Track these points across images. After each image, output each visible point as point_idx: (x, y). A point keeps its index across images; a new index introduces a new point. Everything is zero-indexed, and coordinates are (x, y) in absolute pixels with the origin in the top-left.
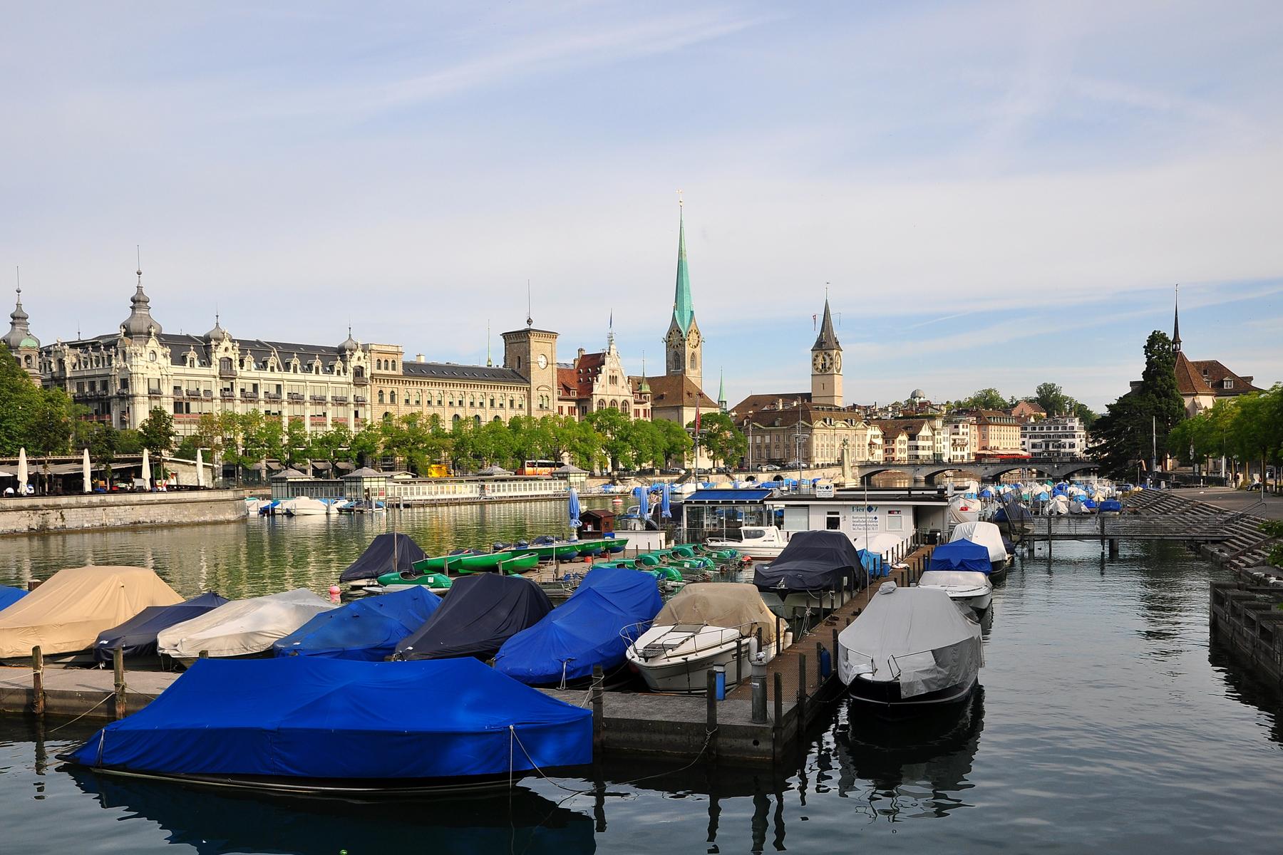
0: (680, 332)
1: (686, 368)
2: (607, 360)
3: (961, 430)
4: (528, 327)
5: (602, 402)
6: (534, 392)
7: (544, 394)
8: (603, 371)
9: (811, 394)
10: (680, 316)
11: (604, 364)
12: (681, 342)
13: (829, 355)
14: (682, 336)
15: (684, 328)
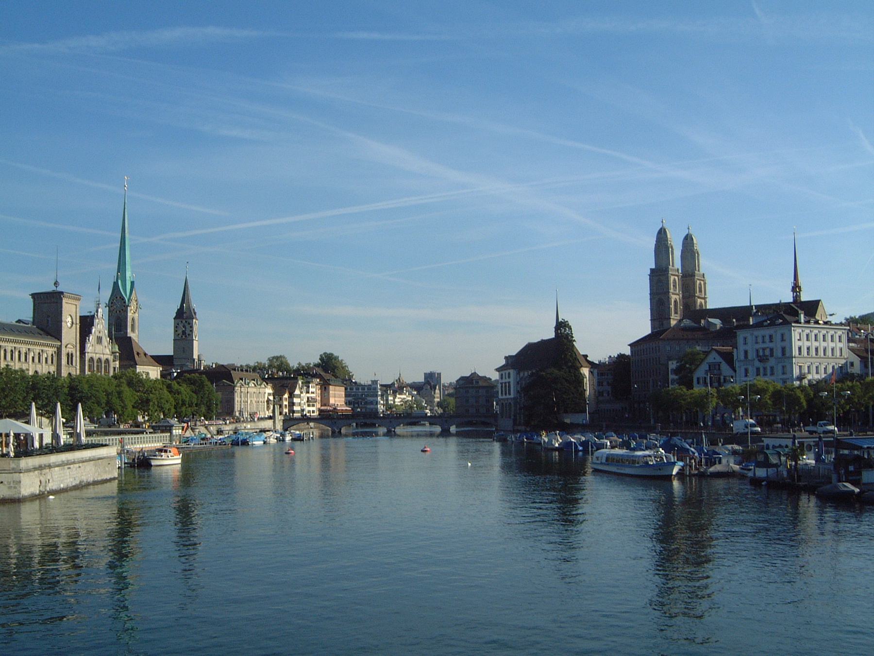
0: (123, 299)
1: (128, 331)
2: (96, 321)
3: (311, 390)
4: (54, 288)
5: (92, 359)
6: (63, 349)
7: (70, 351)
8: (93, 330)
9: (172, 356)
10: (122, 285)
11: (93, 325)
12: (124, 308)
13: (189, 324)
14: (125, 302)
15: (126, 295)
